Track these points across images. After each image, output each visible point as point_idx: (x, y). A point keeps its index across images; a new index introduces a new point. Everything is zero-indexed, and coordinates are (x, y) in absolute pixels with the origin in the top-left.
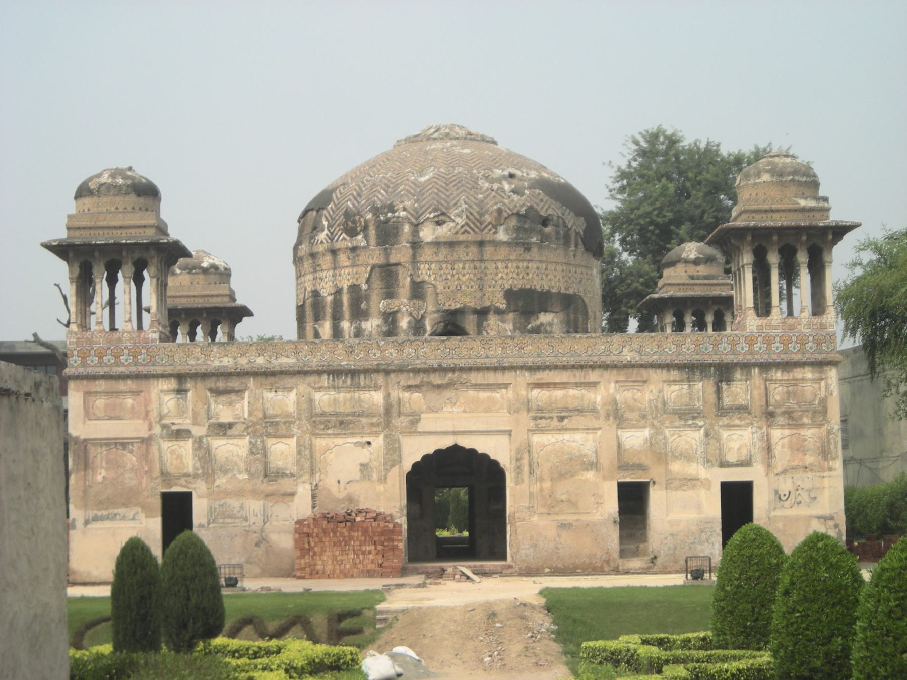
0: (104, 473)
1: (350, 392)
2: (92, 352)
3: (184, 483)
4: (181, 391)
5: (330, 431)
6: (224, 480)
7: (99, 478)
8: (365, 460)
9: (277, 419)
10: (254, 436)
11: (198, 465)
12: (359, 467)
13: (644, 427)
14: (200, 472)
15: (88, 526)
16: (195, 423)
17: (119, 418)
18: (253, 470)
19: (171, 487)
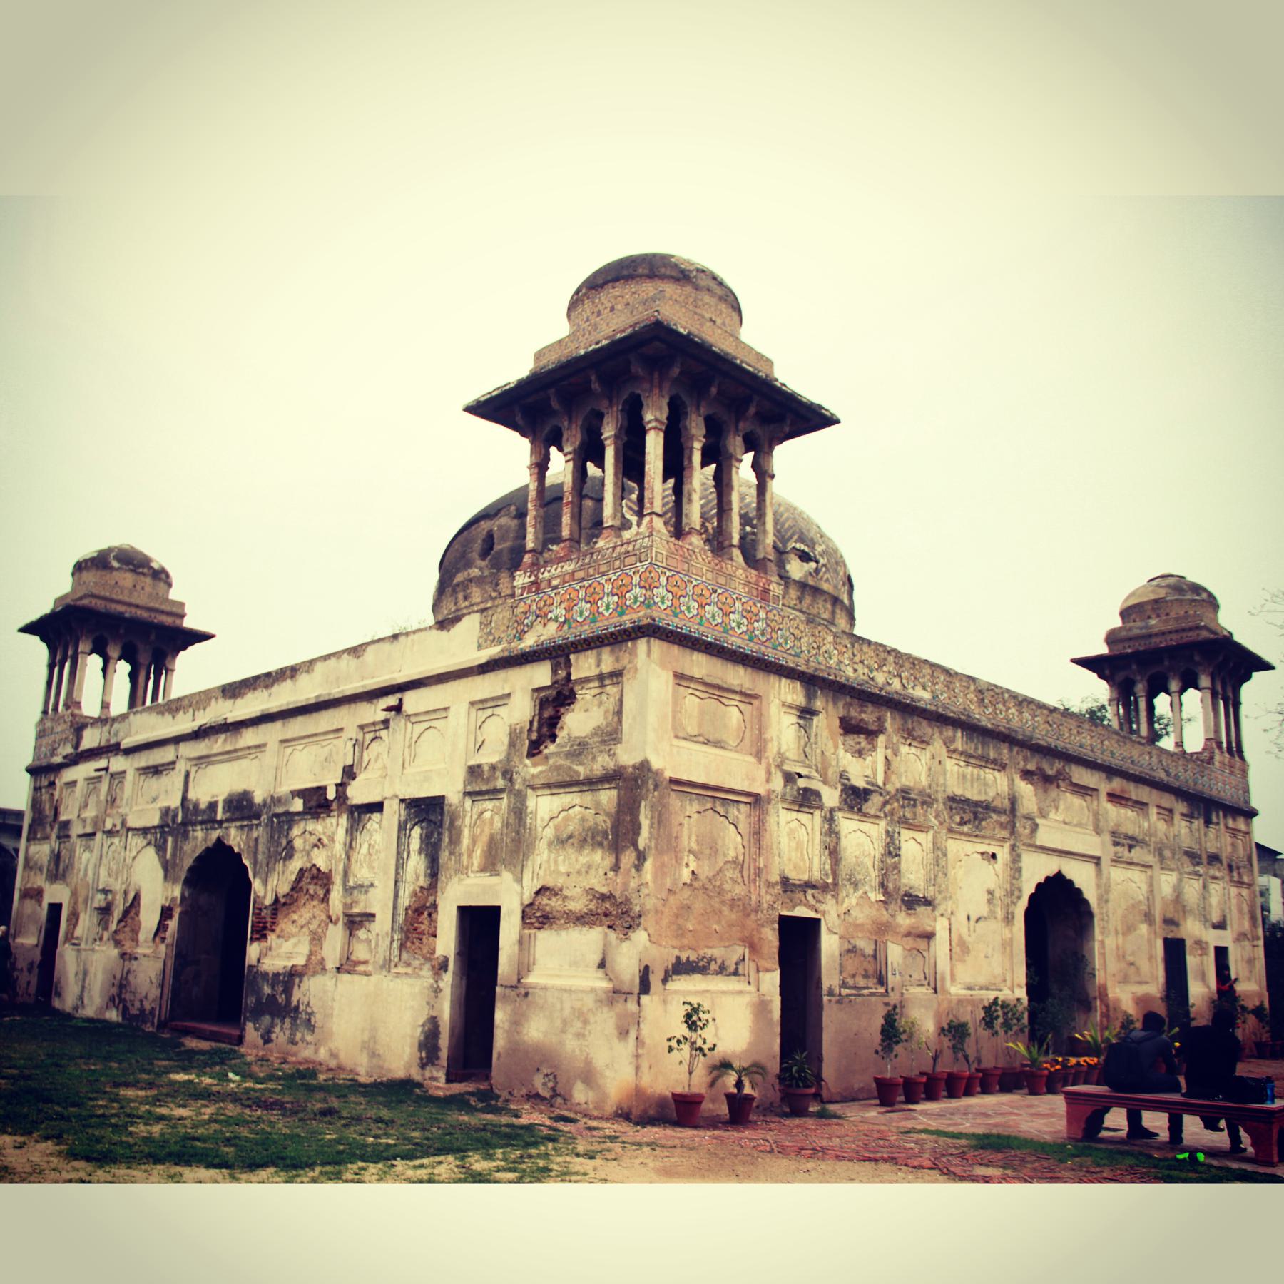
0: (693, 866)
1: (980, 766)
2: (690, 587)
3: (812, 901)
4: (806, 713)
5: (965, 829)
6: (854, 901)
7: (686, 875)
8: (992, 886)
9: (912, 796)
10: (892, 820)
11: (828, 867)
12: (986, 896)
13: (1172, 870)
14: (830, 880)
15: (670, 986)
16: (825, 782)
17: (718, 744)
18: (891, 886)
19: (794, 907)
